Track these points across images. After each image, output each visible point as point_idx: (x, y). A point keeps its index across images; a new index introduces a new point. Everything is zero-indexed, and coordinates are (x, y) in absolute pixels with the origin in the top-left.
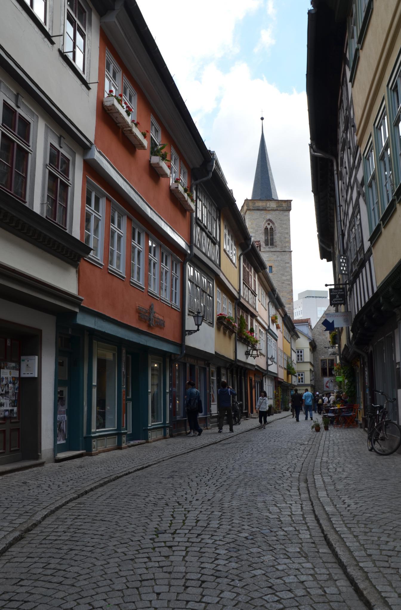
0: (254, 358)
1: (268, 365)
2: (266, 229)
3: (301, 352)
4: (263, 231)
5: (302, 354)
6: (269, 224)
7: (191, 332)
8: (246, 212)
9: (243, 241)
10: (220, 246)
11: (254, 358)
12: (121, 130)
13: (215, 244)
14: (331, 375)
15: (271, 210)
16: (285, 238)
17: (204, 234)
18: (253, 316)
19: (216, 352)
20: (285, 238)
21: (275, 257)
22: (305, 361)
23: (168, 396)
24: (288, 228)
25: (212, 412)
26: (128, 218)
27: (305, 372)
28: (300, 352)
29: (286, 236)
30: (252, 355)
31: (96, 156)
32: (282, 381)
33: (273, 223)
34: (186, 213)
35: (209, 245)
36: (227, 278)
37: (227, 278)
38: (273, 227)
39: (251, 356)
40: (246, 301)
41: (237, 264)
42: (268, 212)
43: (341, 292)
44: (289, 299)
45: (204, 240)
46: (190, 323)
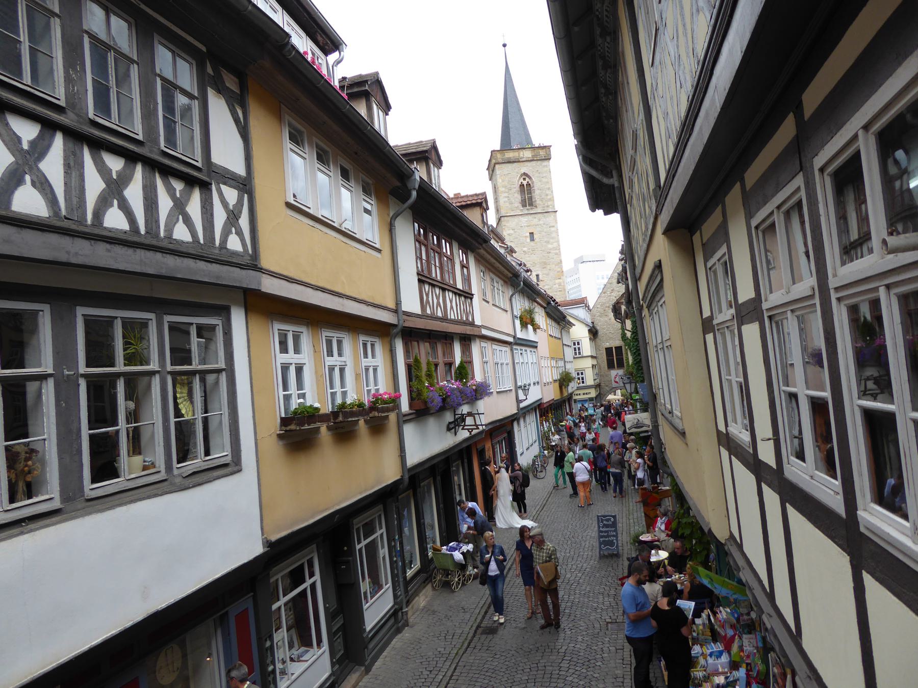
2: (522, 185)
3: (578, 344)
4: (518, 188)
5: (580, 346)
6: (524, 179)
8: (494, 166)
9: (398, 184)
14: (621, 365)
22: (585, 355)
24: (549, 182)
29: (548, 192)
33: (530, 178)
38: (530, 182)
39: (463, 429)
42: (522, 164)
44: (558, 272)
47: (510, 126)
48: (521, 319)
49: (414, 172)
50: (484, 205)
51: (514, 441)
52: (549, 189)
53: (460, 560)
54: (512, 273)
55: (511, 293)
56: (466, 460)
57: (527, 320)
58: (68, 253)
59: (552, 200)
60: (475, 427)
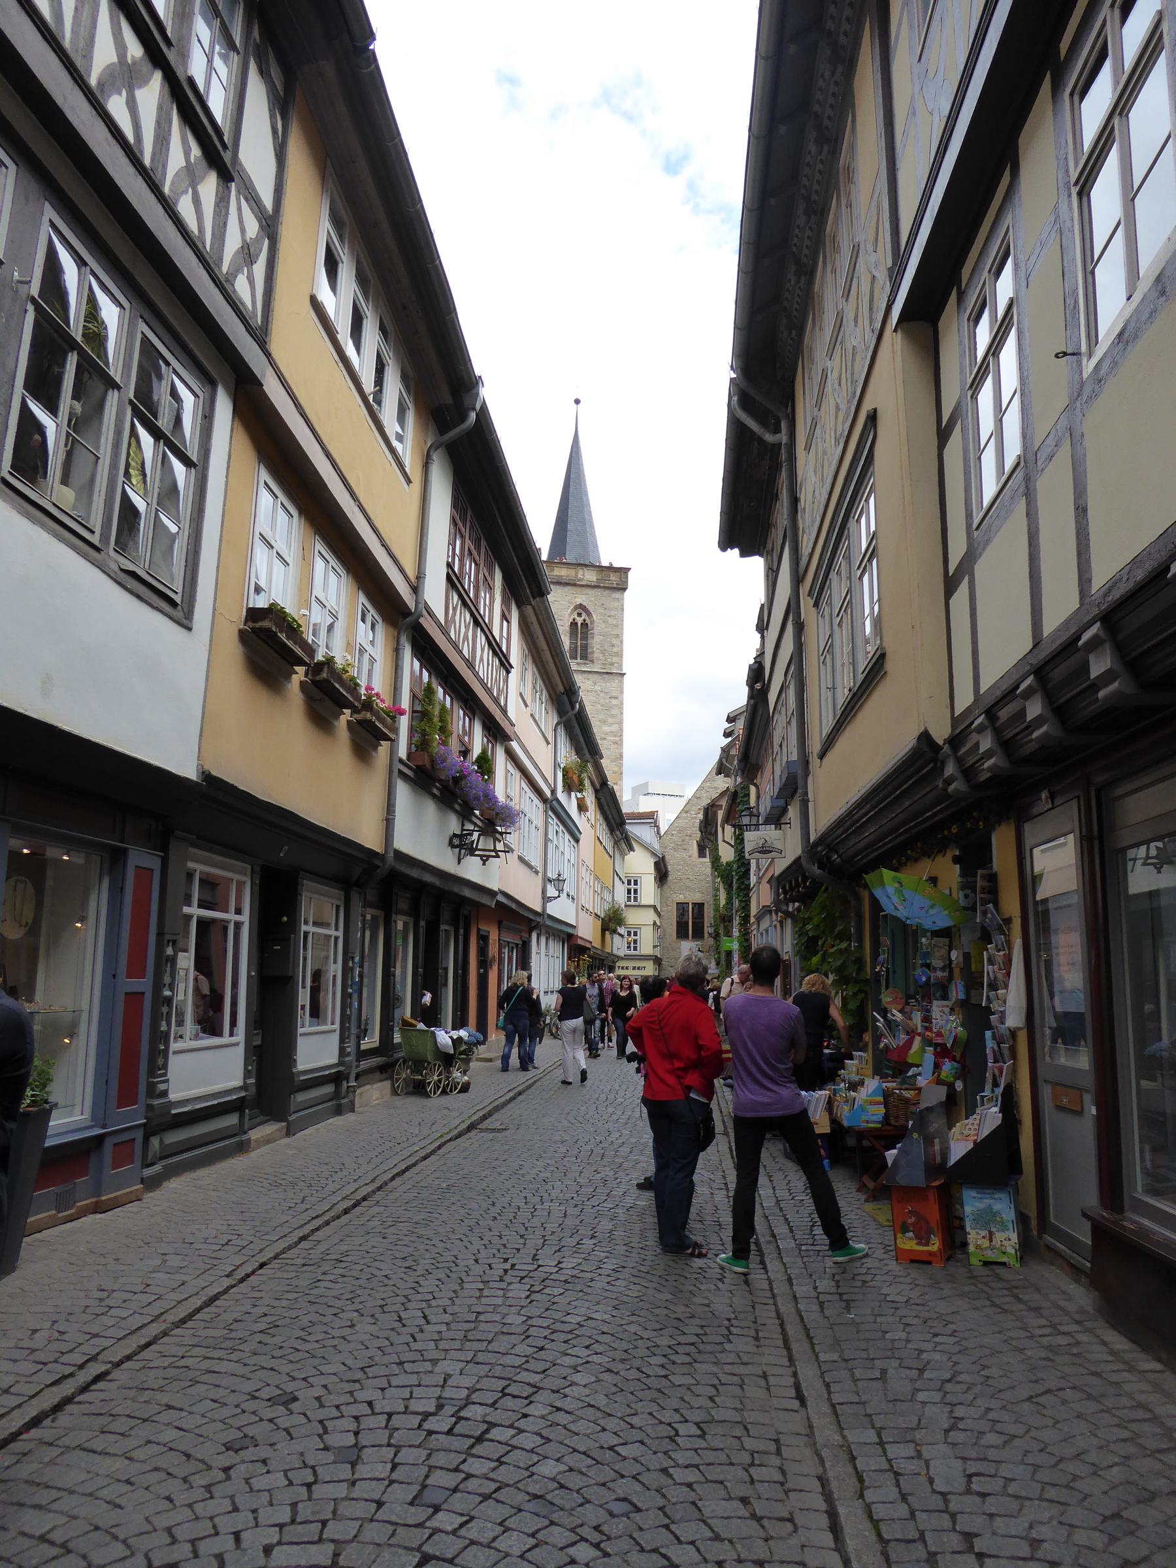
0: (485, 860)
1: (546, 899)
2: (574, 624)
3: (636, 883)
5: (638, 887)
6: (579, 615)
9: (448, 400)
11: (485, 860)
14: (698, 934)
21: (590, 682)
22: (643, 902)
24: (619, 625)
25: (173, 1096)
27: (643, 928)
29: (614, 641)
30: (477, 849)
32: (588, 945)
33: (589, 614)
37: (328, 455)
38: (588, 621)
39: (473, 855)
40: (460, 652)
42: (579, 589)
47: (569, 526)
49: (477, 383)
51: (530, 963)
53: (446, 1046)
54: (565, 688)
56: (462, 931)
58: (65, 98)
59: (619, 654)
60: (494, 854)
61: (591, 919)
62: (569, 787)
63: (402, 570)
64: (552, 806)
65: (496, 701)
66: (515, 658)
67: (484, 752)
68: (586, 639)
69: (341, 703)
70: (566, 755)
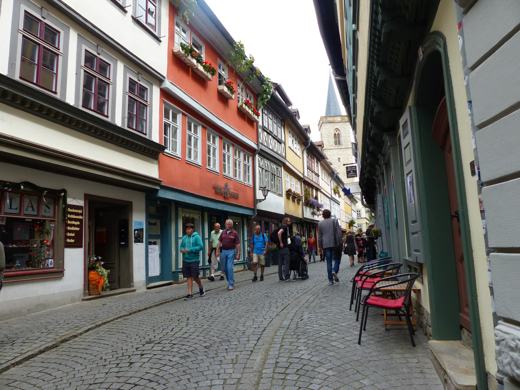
0: (318, 216)
2: (335, 134)
3: (360, 211)
6: (337, 131)
7: (260, 201)
9: (305, 141)
10: (285, 144)
11: (318, 216)
12: (190, 68)
13: (280, 143)
15: (338, 122)
16: (348, 139)
17: (271, 137)
18: (317, 190)
19: (285, 213)
20: (348, 139)
21: (342, 151)
22: (362, 217)
23: (246, 243)
26: (203, 126)
28: (359, 212)
29: (348, 138)
31: (167, 84)
32: (345, 230)
33: (339, 131)
34: (253, 123)
35: (275, 144)
36: (292, 165)
37: (292, 165)
40: (310, 180)
41: (301, 156)
42: (335, 123)
43: (354, 169)
45: (271, 140)
46: (259, 195)
48: (334, 190)
50: (322, 146)
52: (349, 136)
55: (330, 179)
57: (336, 192)
61: (344, 223)
62: (335, 193)
63: (301, 173)
64: (331, 199)
65: (317, 184)
66: (320, 174)
67: (316, 195)
68: (339, 138)
69: (296, 198)
70: (333, 184)
